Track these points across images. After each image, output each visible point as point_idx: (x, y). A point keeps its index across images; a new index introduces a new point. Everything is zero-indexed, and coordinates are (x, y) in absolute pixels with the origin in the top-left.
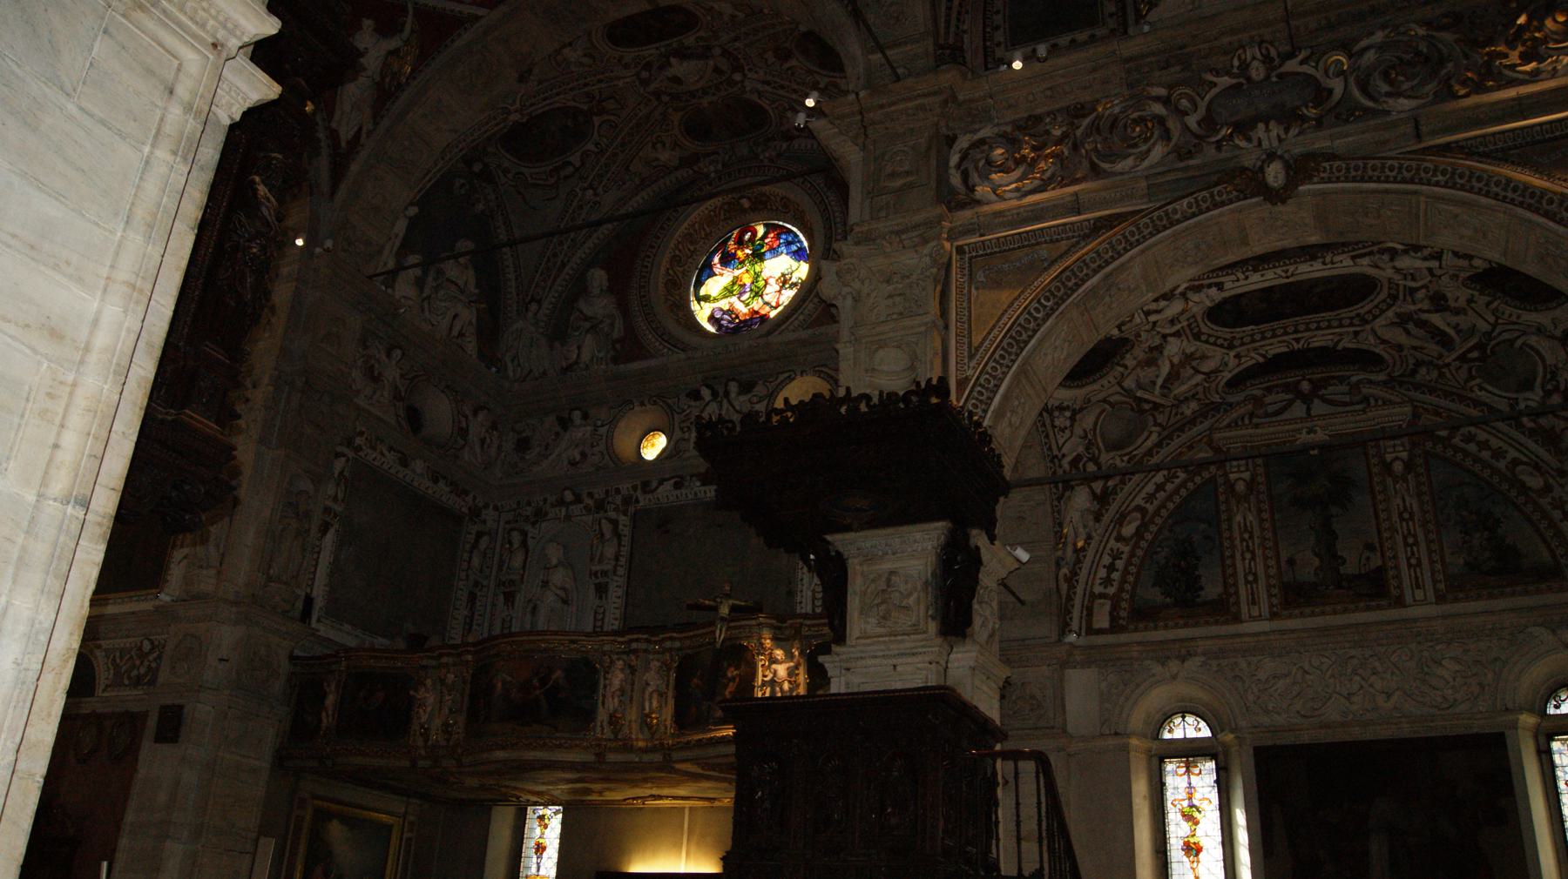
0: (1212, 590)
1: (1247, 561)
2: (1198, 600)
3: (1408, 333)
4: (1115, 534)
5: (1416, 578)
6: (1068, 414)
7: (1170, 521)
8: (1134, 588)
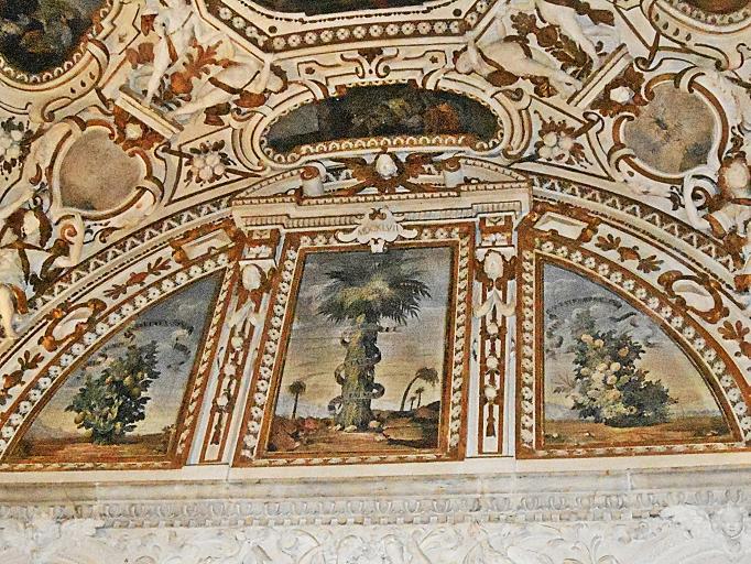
0: (153, 422)
1: (226, 381)
2: (127, 433)
3: (528, 53)
4: (42, 333)
5: (491, 418)
6: (17, 135)
7: (133, 322)
8: (38, 408)
